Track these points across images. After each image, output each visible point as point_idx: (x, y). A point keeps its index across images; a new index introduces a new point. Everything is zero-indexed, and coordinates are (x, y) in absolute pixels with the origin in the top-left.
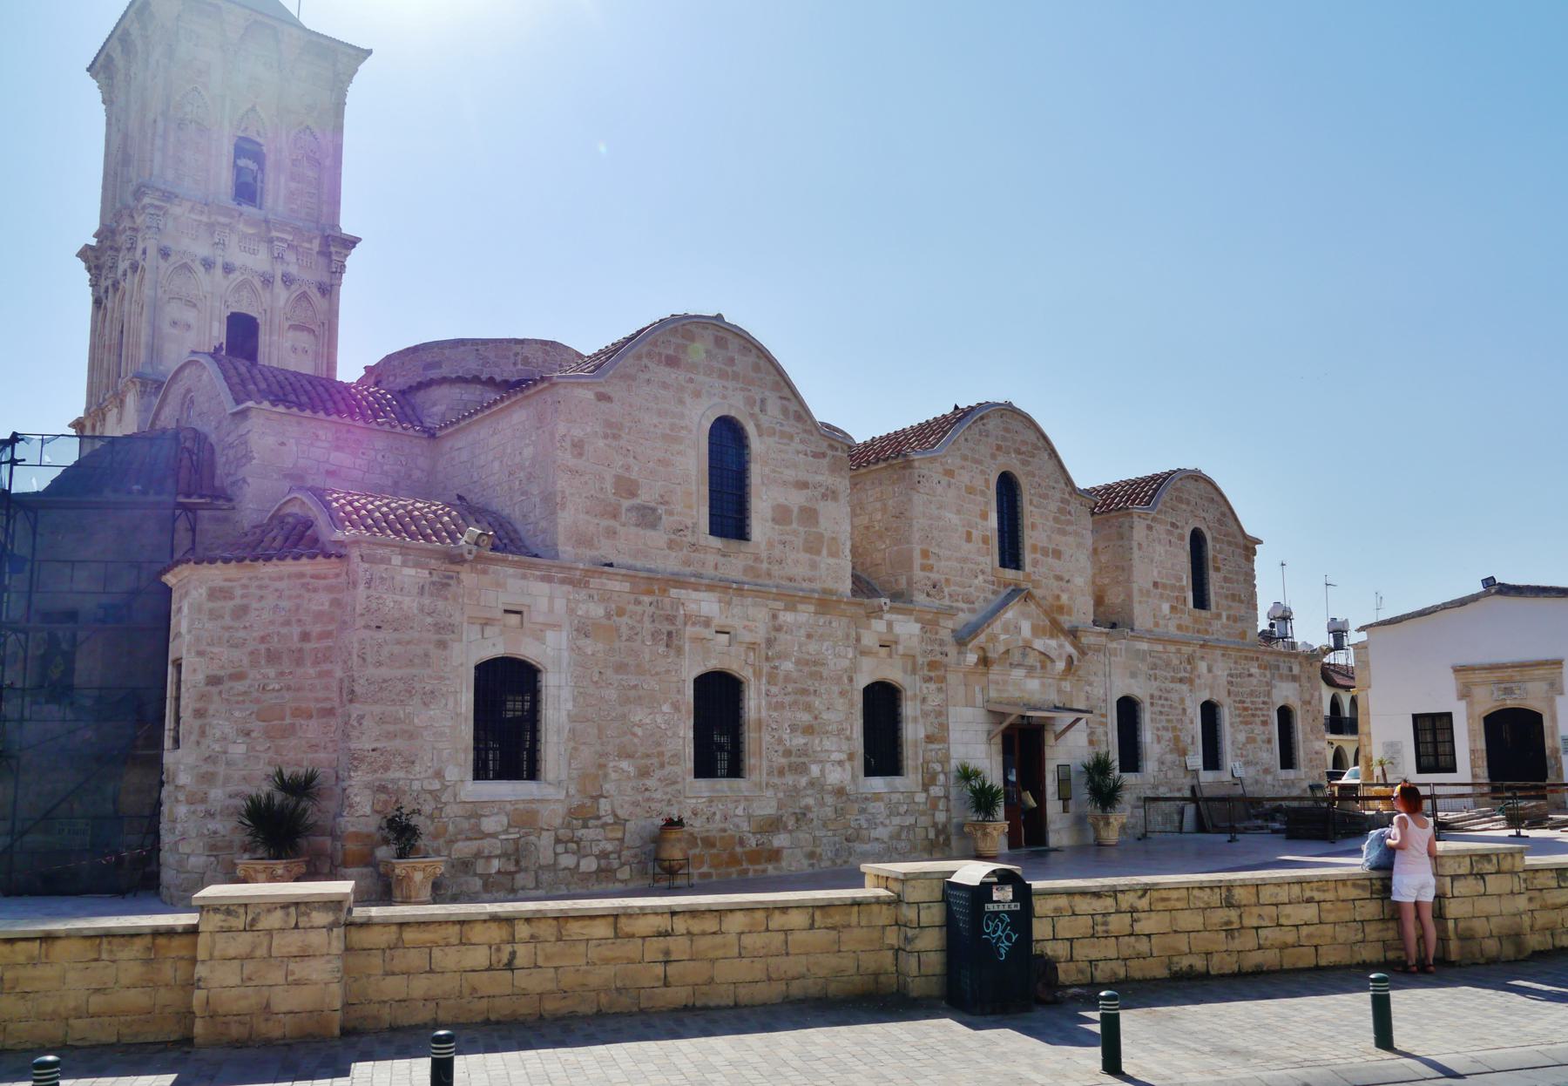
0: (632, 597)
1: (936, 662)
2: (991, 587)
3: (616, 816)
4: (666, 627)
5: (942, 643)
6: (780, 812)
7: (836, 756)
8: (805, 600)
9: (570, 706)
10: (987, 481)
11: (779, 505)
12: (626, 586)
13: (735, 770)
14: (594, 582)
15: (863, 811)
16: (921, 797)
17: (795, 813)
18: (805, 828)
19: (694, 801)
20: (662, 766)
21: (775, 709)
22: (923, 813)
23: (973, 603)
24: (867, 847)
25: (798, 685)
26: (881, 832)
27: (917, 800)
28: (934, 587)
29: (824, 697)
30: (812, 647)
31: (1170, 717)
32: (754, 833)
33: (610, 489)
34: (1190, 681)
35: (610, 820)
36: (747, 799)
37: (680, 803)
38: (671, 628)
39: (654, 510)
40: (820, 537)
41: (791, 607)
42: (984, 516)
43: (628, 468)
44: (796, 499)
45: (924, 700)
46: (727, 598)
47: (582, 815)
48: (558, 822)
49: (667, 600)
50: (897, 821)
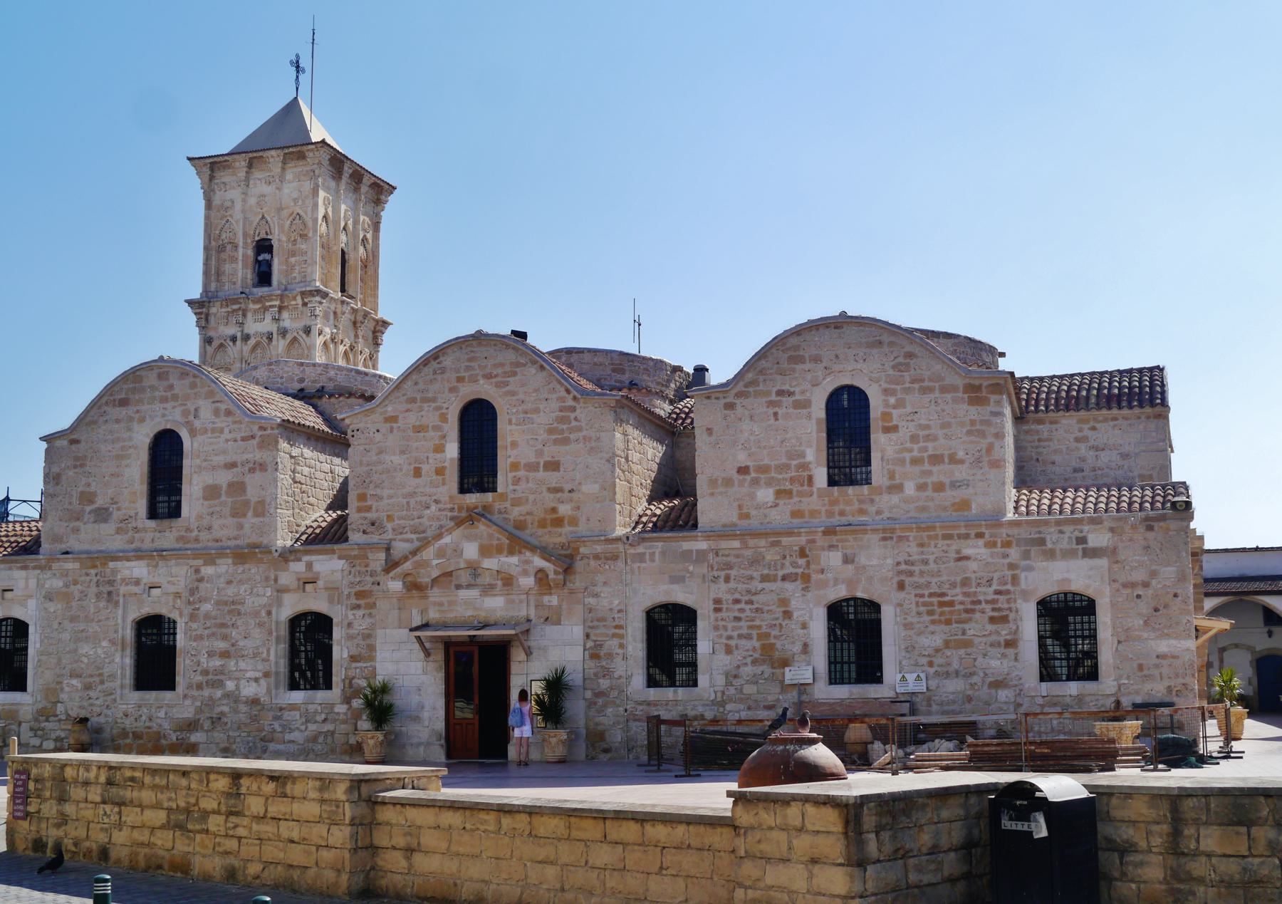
0: (84, 571)
1: (364, 591)
2: (449, 514)
3: (69, 715)
4: (106, 589)
5: (373, 574)
6: (198, 717)
7: (249, 674)
8: (221, 553)
9: (38, 645)
10: (444, 418)
11: (208, 486)
12: (77, 565)
13: (168, 683)
14: (55, 566)
15: (276, 718)
16: (341, 709)
17: (212, 718)
18: (219, 728)
19: (125, 706)
20: (102, 682)
21: (195, 640)
22: (345, 722)
23: (424, 532)
24: (281, 747)
25: (218, 621)
26: (296, 736)
27: (336, 710)
28: (373, 524)
29: (240, 628)
30: (230, 591)
31: (757, 623)
32: (175, 731)
33: (75, 501)
34: (806, 578)
35: (63, 717)
36: (168, 706)
37: (116, 707)
38: (111, 589)
39: (107, 509)
40: (247, 503)
41: (211, 561)
42: (440, 449)
43: (89, 485)
44: (223, 478)
45: (350, 625)
46: (154, 563)
47: (45, 714)
48: (29, 717)
49: (108, 570)
50: (312, 727)
